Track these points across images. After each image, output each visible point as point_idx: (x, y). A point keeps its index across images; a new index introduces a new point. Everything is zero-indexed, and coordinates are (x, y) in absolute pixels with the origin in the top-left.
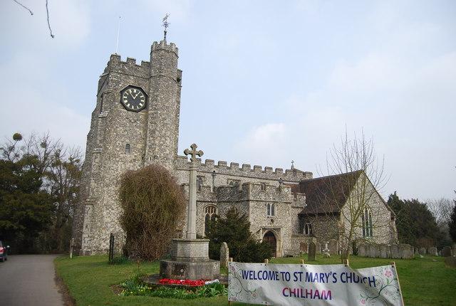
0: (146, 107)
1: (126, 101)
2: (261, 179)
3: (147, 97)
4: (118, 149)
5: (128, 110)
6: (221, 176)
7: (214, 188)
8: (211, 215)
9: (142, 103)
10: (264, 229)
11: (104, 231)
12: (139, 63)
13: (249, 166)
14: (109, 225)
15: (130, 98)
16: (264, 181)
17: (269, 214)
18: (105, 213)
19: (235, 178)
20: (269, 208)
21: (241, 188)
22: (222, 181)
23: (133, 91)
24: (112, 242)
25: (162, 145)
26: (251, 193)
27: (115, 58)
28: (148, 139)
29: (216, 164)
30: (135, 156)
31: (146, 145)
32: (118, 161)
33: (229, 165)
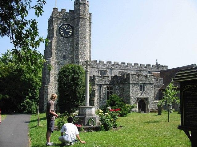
0: (73, 35)
1: (62, 32)
3: (73, 29)
5: (64, 37)
7: (111, 77)
8: (110, 92)
9: (71, 33)
10: (138, 98)
12: (68, 11)
15: (64, 30)
19: (123, 71)
20: (141, 86)
21: (125, 77)
22: (116, 73)
23: (65, 26)
25: (82, 55)
26: (130, 79)
27: (55, 9)
29: (113, 63)
31: (74, 55)
33: (120, 64)
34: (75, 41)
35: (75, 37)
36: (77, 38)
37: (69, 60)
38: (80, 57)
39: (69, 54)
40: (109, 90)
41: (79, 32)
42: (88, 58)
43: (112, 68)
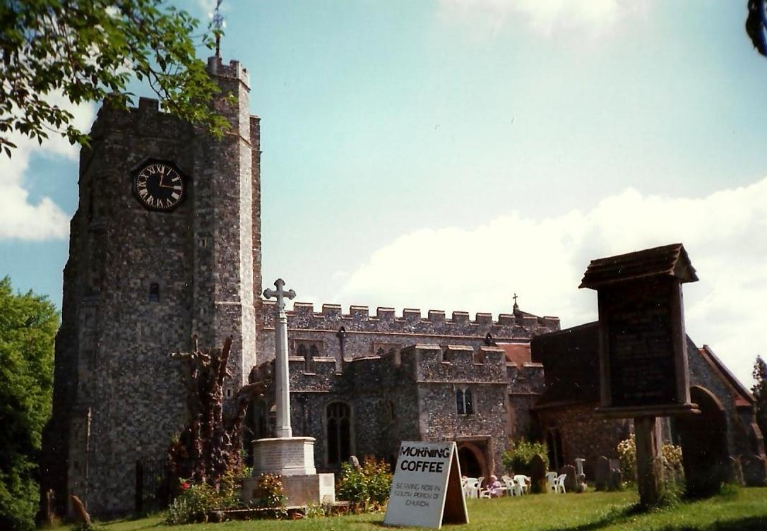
0: (185, 196)
3: (186, 180)
7: (344, 363)
8: (339, 421)
9: (178, 192)
11: (113, 473)
14: (123, 458)
17: (460, 412)
18: (112, 434)
25: (227, 280)
28: (196, 270)
34: (197, 224)
36: (203, 216)
37: (172, 304)
38: (218, 287)
39: (174, 279)
40: (335, 415)
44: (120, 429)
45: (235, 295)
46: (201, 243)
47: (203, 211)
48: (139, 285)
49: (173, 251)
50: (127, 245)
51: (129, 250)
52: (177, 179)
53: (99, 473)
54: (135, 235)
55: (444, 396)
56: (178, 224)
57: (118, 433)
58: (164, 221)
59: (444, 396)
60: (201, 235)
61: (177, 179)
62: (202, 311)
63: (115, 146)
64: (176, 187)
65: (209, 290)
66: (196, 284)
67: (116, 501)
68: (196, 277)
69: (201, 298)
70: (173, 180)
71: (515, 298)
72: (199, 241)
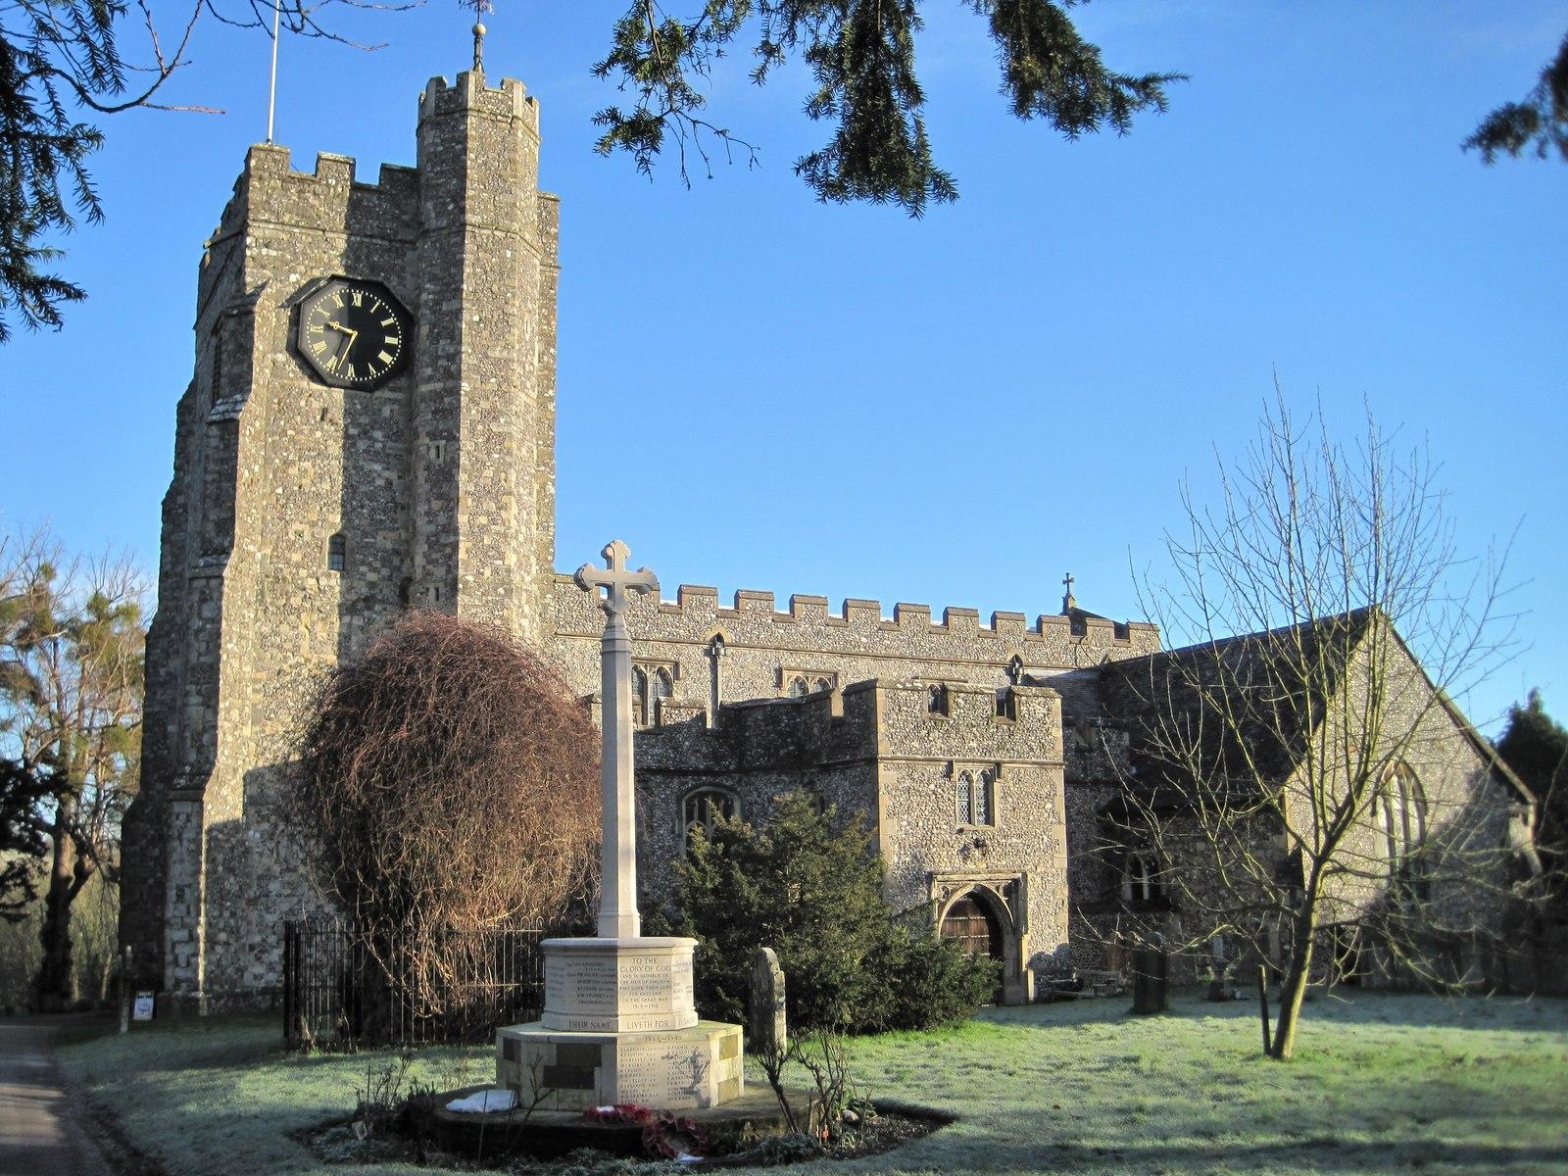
0: (406, 363)
2: (928, 661)
4: (296, 557)
6: (750, 654)
9: (391, 349)
11: (254, 916)
13: (872, 606)
14: (274, 887)
16: (943, 671)
21: (837, 709)
24: (292, 961)
25: (483, 529)
26: (882, 727)
28: (422, 508)
30: (372, 585)
32: (298, 612)
35: (424, 388)
36: (437, 396)
37: (372, 577)
38: (462, 547)
41: (460, 343)
42: (533, 559)
43: (719, 638)
44: (265, 826)
45: (500, 562)
46: (433, 453)
47: (439, 386)
48: (307, 537)
49: (377, 467)
50: (285, 454)
51: (287, 463)
52: (390, 321)
53: (227, 914)
54: (301, 432)
55: (932, 787)
56: (386, 412)
57: (262, 836)
58: (359, 407)
59: (932, 787)
60: (434, 436)
61: (390, 321)
62: (432, 592)
63: (264, 251)
64: (389, 340)
65: (448, 550)
66: (422, 539)
67: (258, 969)
68: (421, 522)
69: (429, 567)
70: (384, 323)
71: (1067, 582)
72: (429, 449)
